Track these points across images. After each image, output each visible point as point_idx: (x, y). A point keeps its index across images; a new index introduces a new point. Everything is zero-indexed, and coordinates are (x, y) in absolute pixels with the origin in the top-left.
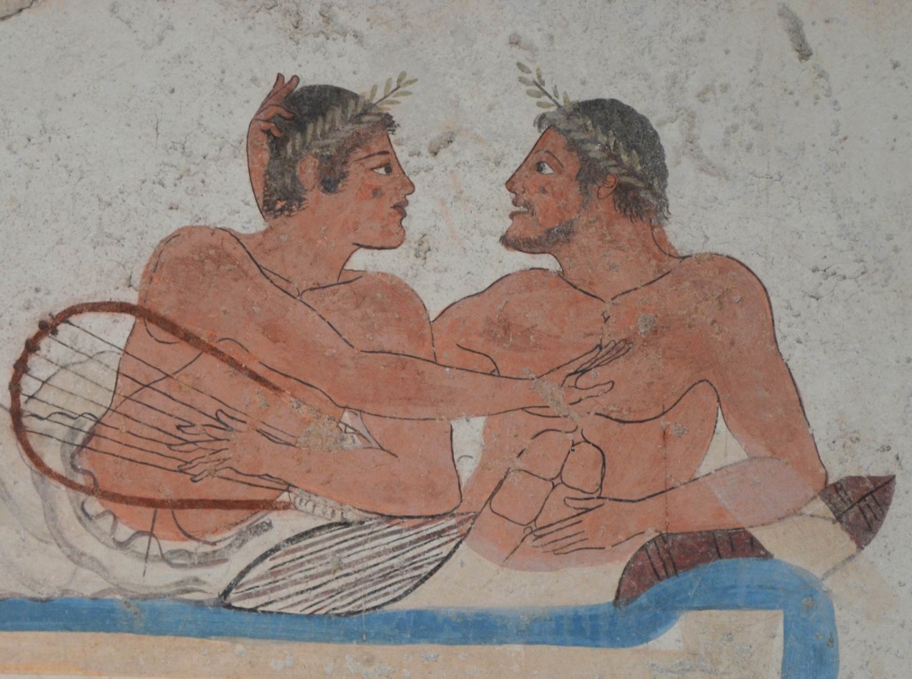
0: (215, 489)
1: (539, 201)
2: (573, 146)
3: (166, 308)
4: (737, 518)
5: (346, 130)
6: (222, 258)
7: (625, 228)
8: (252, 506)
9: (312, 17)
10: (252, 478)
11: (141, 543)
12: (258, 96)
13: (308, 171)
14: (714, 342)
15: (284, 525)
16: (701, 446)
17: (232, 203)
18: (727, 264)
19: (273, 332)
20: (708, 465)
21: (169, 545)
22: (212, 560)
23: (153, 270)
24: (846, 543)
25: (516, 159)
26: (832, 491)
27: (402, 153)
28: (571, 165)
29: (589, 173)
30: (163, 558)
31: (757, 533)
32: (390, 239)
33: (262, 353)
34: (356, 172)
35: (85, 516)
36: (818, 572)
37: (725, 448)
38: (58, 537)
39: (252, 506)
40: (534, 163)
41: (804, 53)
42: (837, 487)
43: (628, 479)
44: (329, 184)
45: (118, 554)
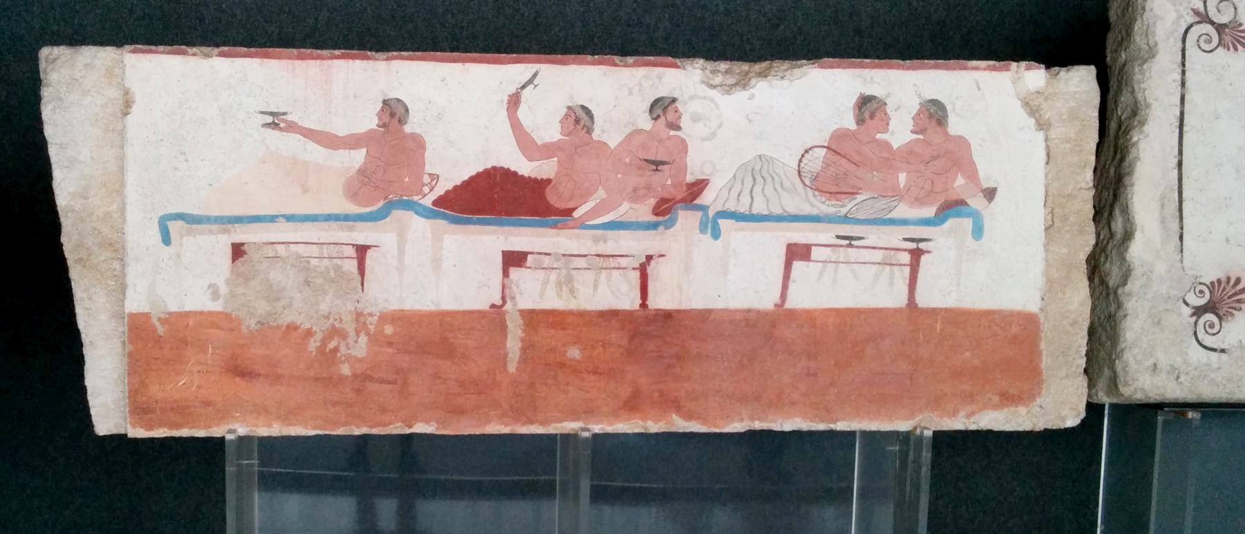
2: (928, 110)
3: (833, 147)
4: (963, 197)
5: (875, 105)
7: (939, 129)
8: (853, 193)
10: (853, 187)
14: (957, 157)
15: (860, 198)
16: (954, 180)
17: (850, 123)
18: (961, 138)
19: (859, 152)
23: (831, 138)
24: (986, 202)
25: (914, 112)
26: (983, 191)
29: (931, 116)
32: (886, 131)
33: (856, 158)
37: (960, 181)
38: (808, 200)
39: (853, 193)
40: (918, 114)
41: (979, 89)
43: (938, 188)
44: (872, 118)
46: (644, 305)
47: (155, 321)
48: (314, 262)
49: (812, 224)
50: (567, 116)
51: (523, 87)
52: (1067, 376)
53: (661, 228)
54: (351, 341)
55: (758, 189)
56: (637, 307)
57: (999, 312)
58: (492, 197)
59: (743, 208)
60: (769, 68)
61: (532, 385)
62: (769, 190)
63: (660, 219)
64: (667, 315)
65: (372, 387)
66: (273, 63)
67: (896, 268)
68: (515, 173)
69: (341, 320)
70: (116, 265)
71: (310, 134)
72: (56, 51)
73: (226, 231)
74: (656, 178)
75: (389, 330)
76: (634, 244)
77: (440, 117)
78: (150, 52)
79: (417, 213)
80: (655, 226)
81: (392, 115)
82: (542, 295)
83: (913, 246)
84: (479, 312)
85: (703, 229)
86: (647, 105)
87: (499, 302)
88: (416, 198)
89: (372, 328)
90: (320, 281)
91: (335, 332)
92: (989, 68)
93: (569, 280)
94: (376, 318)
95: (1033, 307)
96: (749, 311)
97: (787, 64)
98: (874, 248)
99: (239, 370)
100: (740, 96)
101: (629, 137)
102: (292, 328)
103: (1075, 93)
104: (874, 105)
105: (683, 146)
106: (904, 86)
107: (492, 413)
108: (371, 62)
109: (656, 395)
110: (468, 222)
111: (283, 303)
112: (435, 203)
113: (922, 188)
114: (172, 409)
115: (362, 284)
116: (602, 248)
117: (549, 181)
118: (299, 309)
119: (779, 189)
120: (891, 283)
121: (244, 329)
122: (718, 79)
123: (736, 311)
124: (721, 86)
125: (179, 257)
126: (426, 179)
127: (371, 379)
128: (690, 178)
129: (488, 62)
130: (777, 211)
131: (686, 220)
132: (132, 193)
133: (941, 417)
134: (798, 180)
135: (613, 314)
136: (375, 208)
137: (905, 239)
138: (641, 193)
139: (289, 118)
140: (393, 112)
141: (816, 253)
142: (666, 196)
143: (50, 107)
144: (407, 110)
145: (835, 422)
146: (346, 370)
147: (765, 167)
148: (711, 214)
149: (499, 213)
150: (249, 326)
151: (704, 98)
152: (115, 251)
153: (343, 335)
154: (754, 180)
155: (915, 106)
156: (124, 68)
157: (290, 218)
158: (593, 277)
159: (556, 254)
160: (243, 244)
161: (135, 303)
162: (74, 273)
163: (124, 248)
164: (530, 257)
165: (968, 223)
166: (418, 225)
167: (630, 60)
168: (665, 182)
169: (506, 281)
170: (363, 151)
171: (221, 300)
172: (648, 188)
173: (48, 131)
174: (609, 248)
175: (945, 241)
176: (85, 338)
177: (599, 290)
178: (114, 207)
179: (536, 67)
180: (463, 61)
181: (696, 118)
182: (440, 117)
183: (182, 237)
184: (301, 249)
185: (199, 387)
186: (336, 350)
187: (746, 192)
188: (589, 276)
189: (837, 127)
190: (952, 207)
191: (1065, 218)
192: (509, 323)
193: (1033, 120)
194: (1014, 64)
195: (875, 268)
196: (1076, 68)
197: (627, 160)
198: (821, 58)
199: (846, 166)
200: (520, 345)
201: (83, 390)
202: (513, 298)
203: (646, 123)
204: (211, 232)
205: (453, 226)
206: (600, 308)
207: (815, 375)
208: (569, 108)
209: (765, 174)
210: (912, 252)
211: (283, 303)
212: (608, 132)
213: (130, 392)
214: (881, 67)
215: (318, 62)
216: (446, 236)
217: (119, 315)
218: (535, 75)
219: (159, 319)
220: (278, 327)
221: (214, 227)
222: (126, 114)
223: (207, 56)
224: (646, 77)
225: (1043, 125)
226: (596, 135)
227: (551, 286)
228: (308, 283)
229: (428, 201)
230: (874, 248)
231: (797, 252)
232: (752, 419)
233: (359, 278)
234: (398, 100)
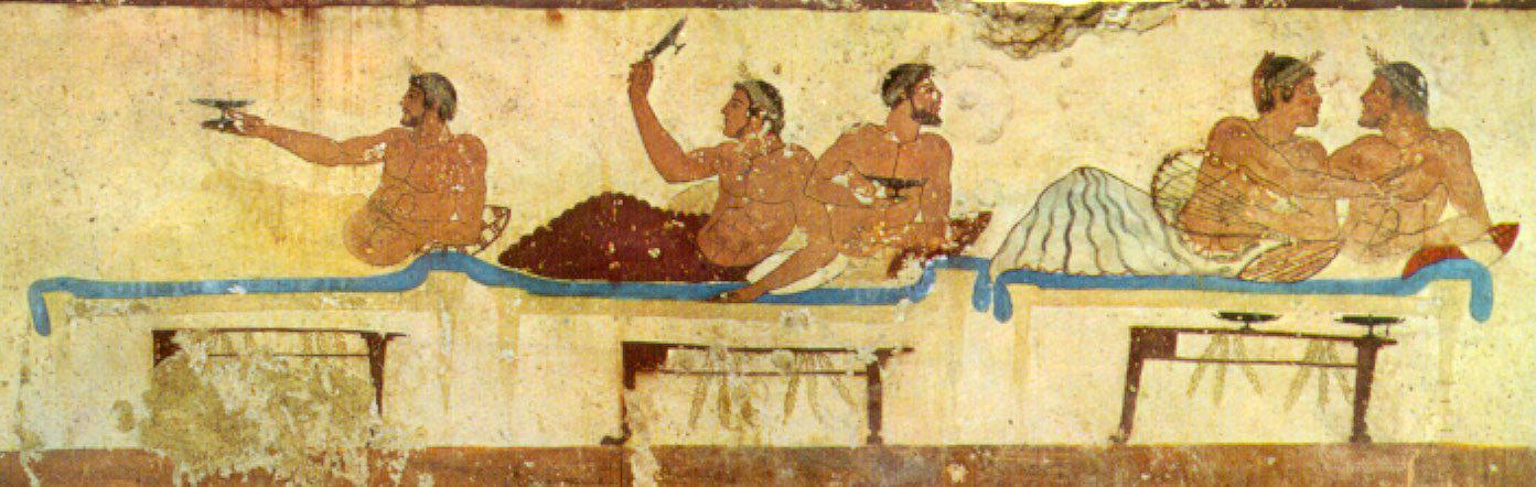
1: (1376, 106)
4: (1453, 241)
6: (1239, 130)
11: (1205, 253)
12: (1256, 62)
17: (1244, 106)
21: (1218, 253)
22: (1233, 259)
24: (1494, 250)
25: (1366, 86)
26: (1491, 230)
30: (1215, 259)
31: (1465, 250)
32: (1313, 120)
34: (1298, 95)
35: (1181, 240)
36: (1486, 264)
42: (1495, 229)
43: (1410, 222)
44: (1286, 99)
45: (1195, 257)
46: (874, 439)
51: (658, 50)
53: (905, 302)
55: (1078, 231)
59: (1052, 261)
62: (1099, 230)
67: (1331, 372)
68: (645, 205)
69: (343, 465)
76: (857, 330)
81: (428, 104)
83: (1359, 331)
86: (876, 79)
87: (616, 434)
104: (1288, 78)
112: (506, 258)
115: (379, 403)
117: (705, 217)
124: (1012, 43)
130: (1115, 268)
136: (399, 268)
137: (1347, 320)
139: (251, 111)
140: (429, 98)
141: (1184, 344)
144: (453, 95)
147: (1092, 190)
148: (995, 273)
154: (1073, 212)
157: (254, 287)
158: (784, 388)
160: (173, 333)
164: (671, 353)
165: (1464, 289)
169: (631, 396)
171: (136, 432)
177: (796, 412)
187: (1058, 234)
188: (779, 387)
190: (1432, 259)
192: (635, 470)
203: (875, 111)
205: (534, 302)
208: (738, 87)
209: (1092, 202)
210: (1358, 342)
218: (676, 30)
219: (32, 463)
221: (125, 304)
227: (711, 401)
229: (491, 256)
231: (1150, 344)
233: (375, 390)
234: (440, 79)
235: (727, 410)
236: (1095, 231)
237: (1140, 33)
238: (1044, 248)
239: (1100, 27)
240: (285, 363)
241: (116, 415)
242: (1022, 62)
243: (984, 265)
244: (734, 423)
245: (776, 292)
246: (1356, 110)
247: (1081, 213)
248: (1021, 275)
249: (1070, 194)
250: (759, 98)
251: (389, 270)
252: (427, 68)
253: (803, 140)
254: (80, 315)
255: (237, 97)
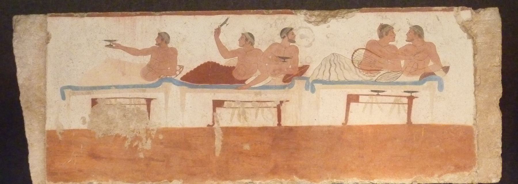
0: (374, 68)
2: (413, 30)
3: (369, 49)
4: (433, 71)
7: (420, 39)
8: (378, 70)
9: (384, 17)
13: (384, 33)
14: (429, 52)
15: (382, 72)
16: (428, 63)
17: (376, 37)
18: (431, 43)
20: (429, 65)
22: (374, 76)
23: (367, 45)
27: (394, 31)
28: (413, 32)
29: (415, 33)
32: (394, 41)
33: (379, 53)
37: (431, 63)
38: (357, 74)
40: (409, 32)
41: (439, 20)
44: (386, 35)
46: (279, 124)
47: (58, 134)
48: (128, 106)
49: (359, 85)
50: (242, 37)
51: (222, 25)
52: (490, 158)
53: (287, 88)
54: (144, 142)
55: (332, 69)
56: (276, 125)
57: (453, 126)
58: (207, 75)
59: (326, 78)
60: (337, 13)
61: (227, 162)
62: (338, 69)
63: (286, 84)
64: (291, 130)
65: (153, 163)
66: (110, 19)
67: (400, 105)
68: (218, 65)
69: (140, 133)
70: (42, 109)
71: (126, 49)
72: (19, 17)
73: (89, 93)
74: (284, 65)
75: (161, 137)
76: (275, 96)
77: (184, 40)
78: (58, 16)
79: (174, 84)
80: (284, 87)
81: (162, 40)
82: (231, 120)
83: (409, 94)
84: (202, 128)
85: (307, 89)
86: (279, 32)
87: (211, 124)
88: (173, 77)
89: (153, 136)
90: (130, 115)
91: (137, 138)
92: (443, 10)
93: (244, 113)
94: (155, 132)
95: (470, 122)
96: (330, 126)
97: (345, 11)
98: (390, 96)
99: (94, 156)
100: (323, 26)
101: (271, 47)
102: (118, 136)
103: (489, 20)
105: (297, 50)
106: (402, 20)
107: (208, 175)
108: (153, 16)
109: (286, 167)
110: (197, 87)
111: (114, 125)
112: (182, 79)
113: (412, 67)
114: (65, 173)
115: (149, 116)
116: (259, 98)
117: (234, 67)
118: (121, 128)
119: (343, 69)
120: (399, 112)
121: (97, 137)
122: (313, 19)
123: (323, 127)
125: (69, 105)
126: (178, 68)
127: (153, 159)
128: (300, 65)
129: (206, 14)
130: (342, 79)
131: (298, 84)
132: (50, 77)
133: (426, 177)
134: (352, 65)
135: (263, 129)
136: (154, 82)
137: (405, 92)
138: (276, 72)
139: (117, 42)
140: (163, 38)
141: (361, 98)
142: (289, 73)
143: (16, 41)
144: (169, 37)
145: (373, 179)
146: (141, 155)
147: (336, 59)
148: (310, 81)
149: (211, 83)
150: (99, 136)
151: (306, 28)
152: (42, 103)
153: (140, 139)
154: (331, 65)
155: (408, 29)
156: (47, 23)
157: (117, 87)
159: (237, 101)
160: (96, 99)
161: (50, 126)
162: (24, 114)
163: (46, 102)
164: (225, 103)
165: (436, 83)
166: (174, 89)
167: (271, 11)
168: (288, 66)
169: (215, 114)
170: (150, 56)
171: (87, 124)
172: (281, 70)
173: (15, 52)
174: (263, 98)
175: (425, 93)
176: (29, 142)
177: (258, 117)
178: (42, 84)
179: (228, 15)
180: (194, 14)
181: (302, 37)
182: (184, 40)
183: (70, 96)
184: (122, 100)
185: (76, 163)
186: (137, 146)
188: (253, 111)
189: (369, 39)
190: (427, 76)
191: (486, 81)
193: (466, 34)
194: (455, 8)
195: (391, 105)
196: (488, 8)
197: (270, 57)
198: (361, 8)
199: (375, 58)
200: (221, 144)
201: (28, 165)
202: (218, 122)
204: (83, 94)
205: (190, 89)
206: (258, 126)
207: (363, 157)
208: (243, 34)
209: (336, 62)
211: (114, 125)
212: (262, 44)
213: (47, 165)
214: (391, 11)
215: (130, 17)
216: (187, 94)
217: (43, 131)
219: (60, 133)
220: (112, 136)
221: (84, 92)
222: (47, 43)
223: (82, 16)
224: (278, 19)
225: (472, 37)
226: (256, 46)
227: (236, 115)
228: (125, 116)
229: (178, 78)
230: (390, 96)
231: (352, 99)
232: (332, 178)
233: (148, 113)
235: (240, 117)
236: (337, 70)
237: (347, 19)
238: (323, 74)
239: (337, 18)
240: (125, 106)
241: (82, 120)
242: (316, 27)
243: (307, 79)
244: (242, 121)
245: (253, 86)
246: (405, 38)
247: (333, 65)
248: (317, 81)
249: (330, 60)
250: (248, 36)
251: (151, 82)
252: (163, 31)
253: (260, 47)
254: (73, 95)
255: (114, 39)
